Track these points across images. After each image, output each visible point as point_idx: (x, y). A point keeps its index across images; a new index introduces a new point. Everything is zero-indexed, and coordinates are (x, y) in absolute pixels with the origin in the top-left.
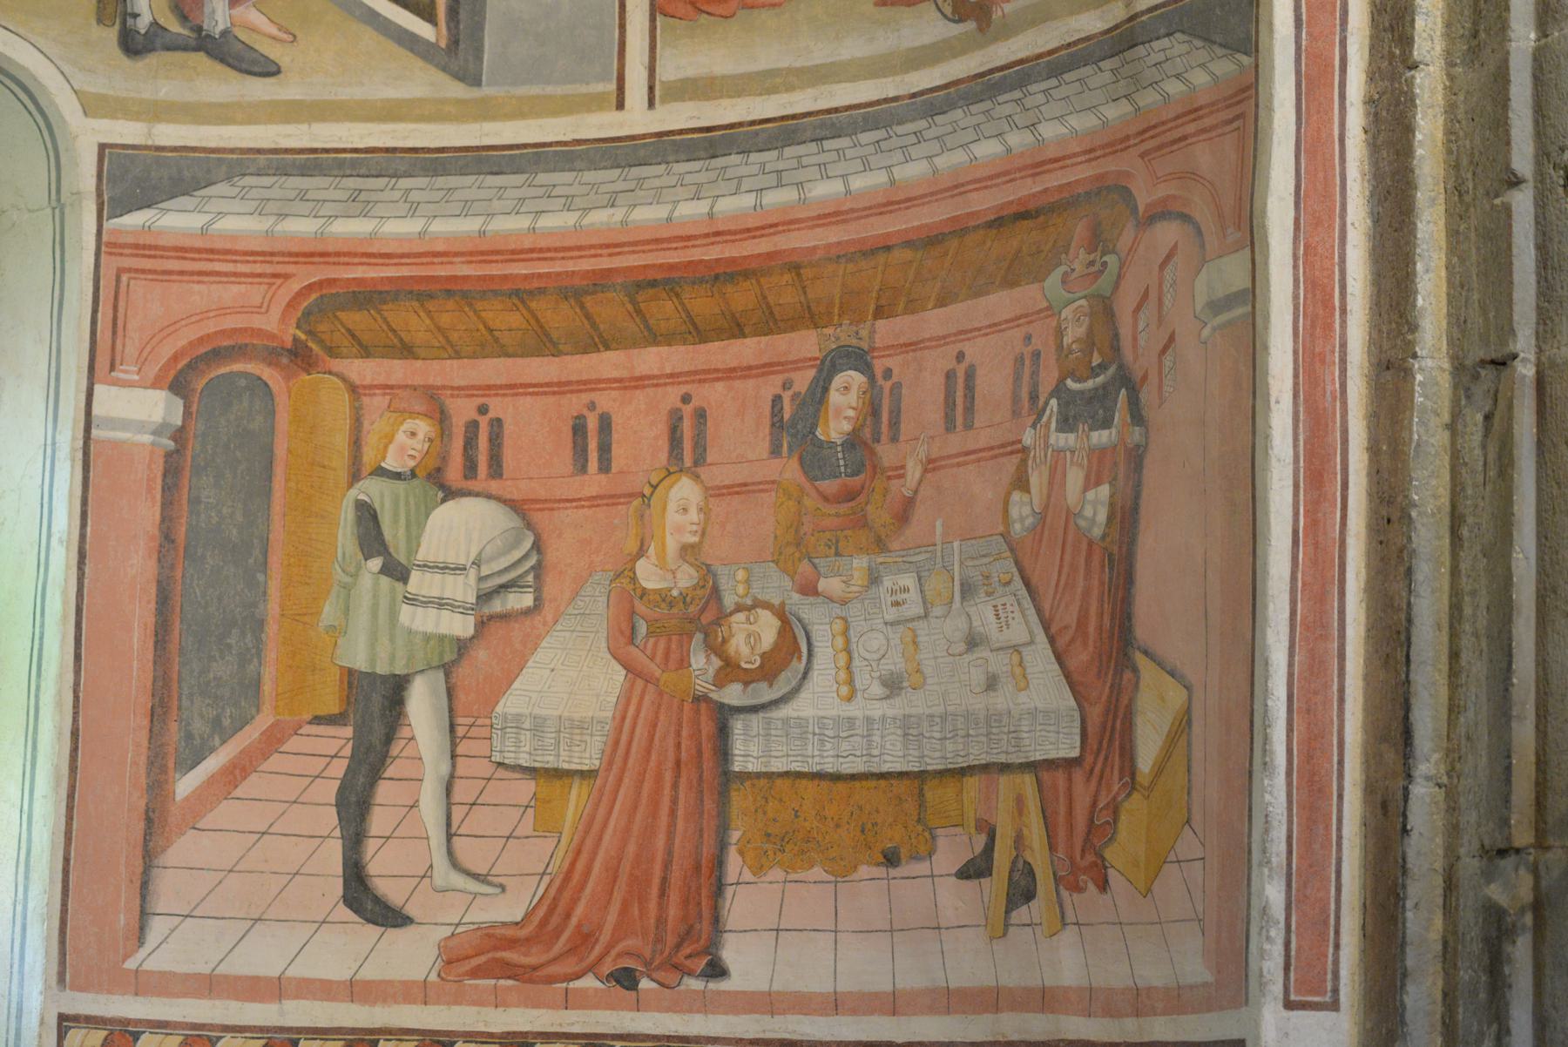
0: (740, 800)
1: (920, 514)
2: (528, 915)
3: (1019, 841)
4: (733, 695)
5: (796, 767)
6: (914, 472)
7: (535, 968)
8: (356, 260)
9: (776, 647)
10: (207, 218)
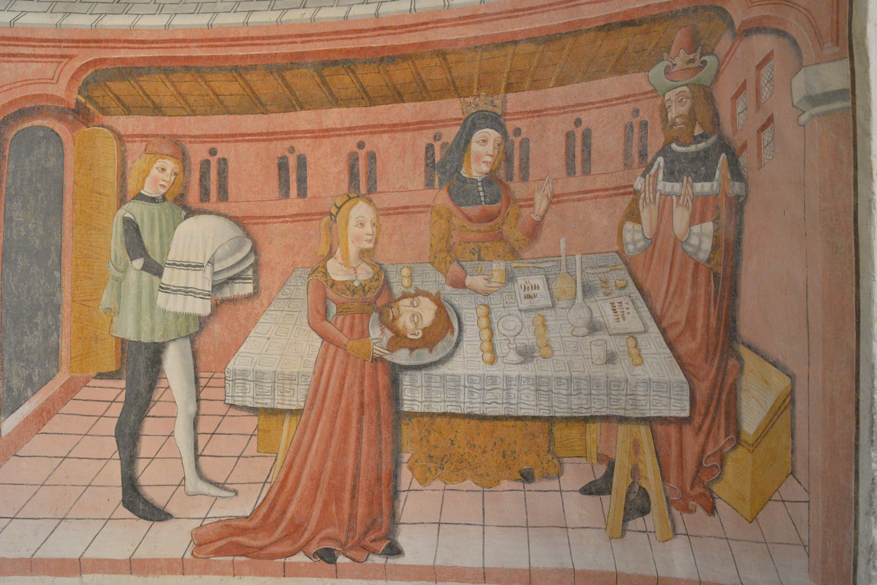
0: (408, 432)
1: (546, 234)
2: (255, 512)
3: (635, 472)
4: (402, 357)
5: (451, 409)
6: (541, 204)
7: (261, 548)
8: (120, 45)
9: (434, 323)
10: (14, 15)
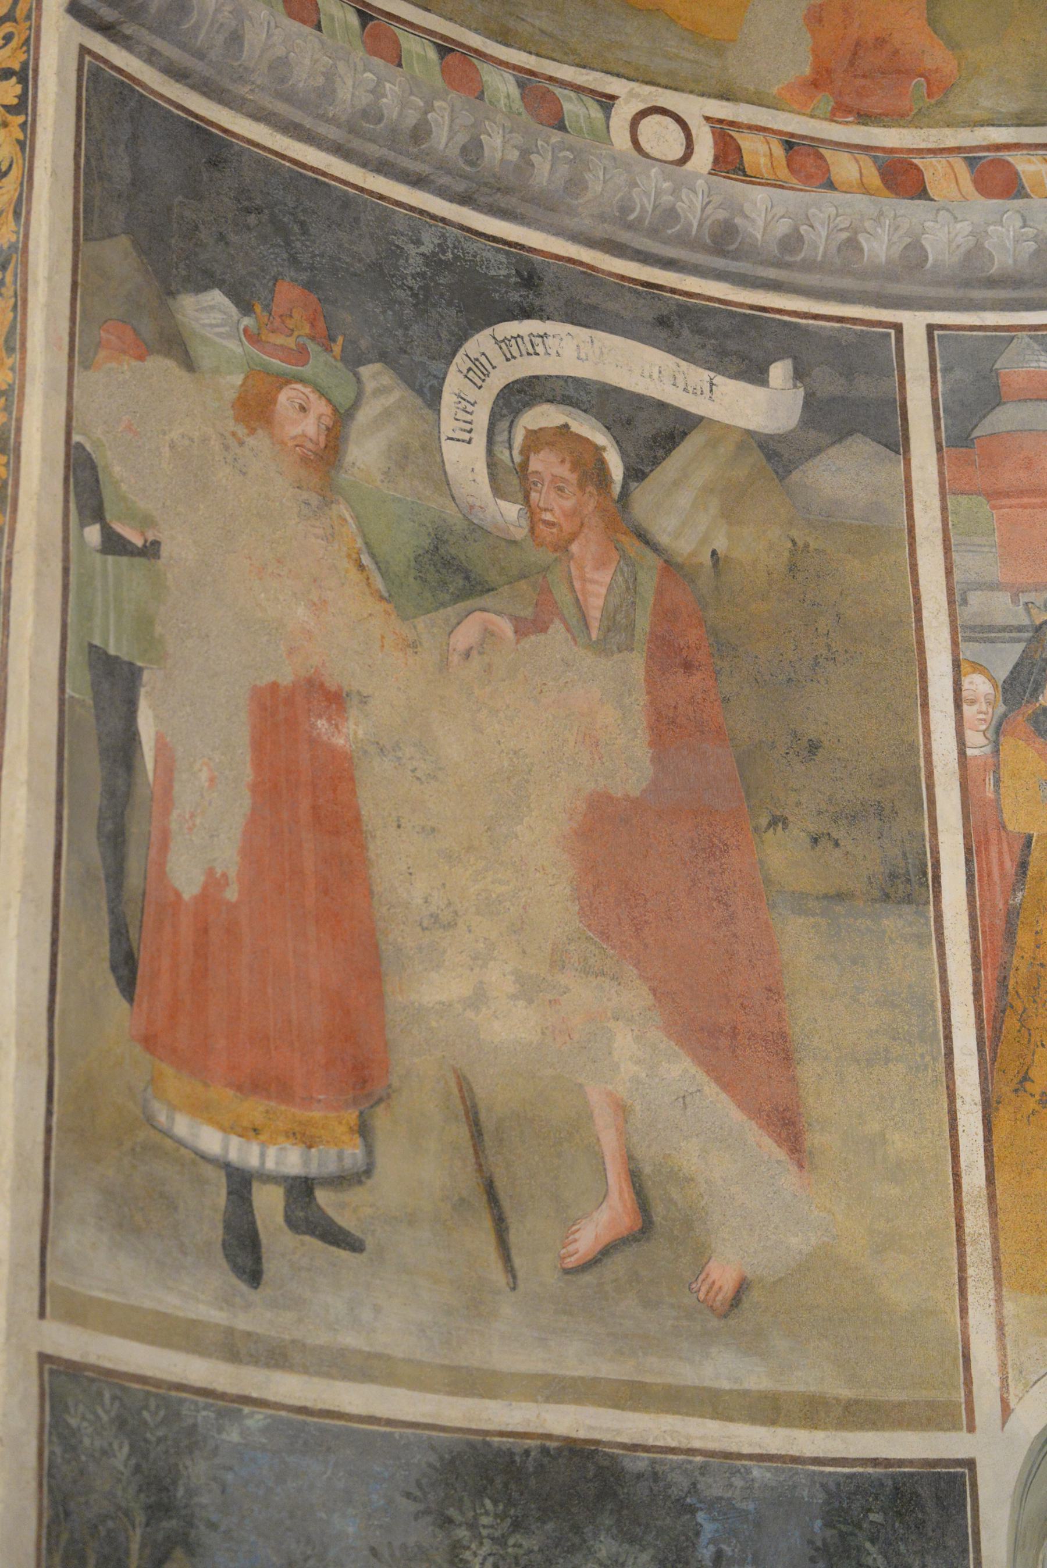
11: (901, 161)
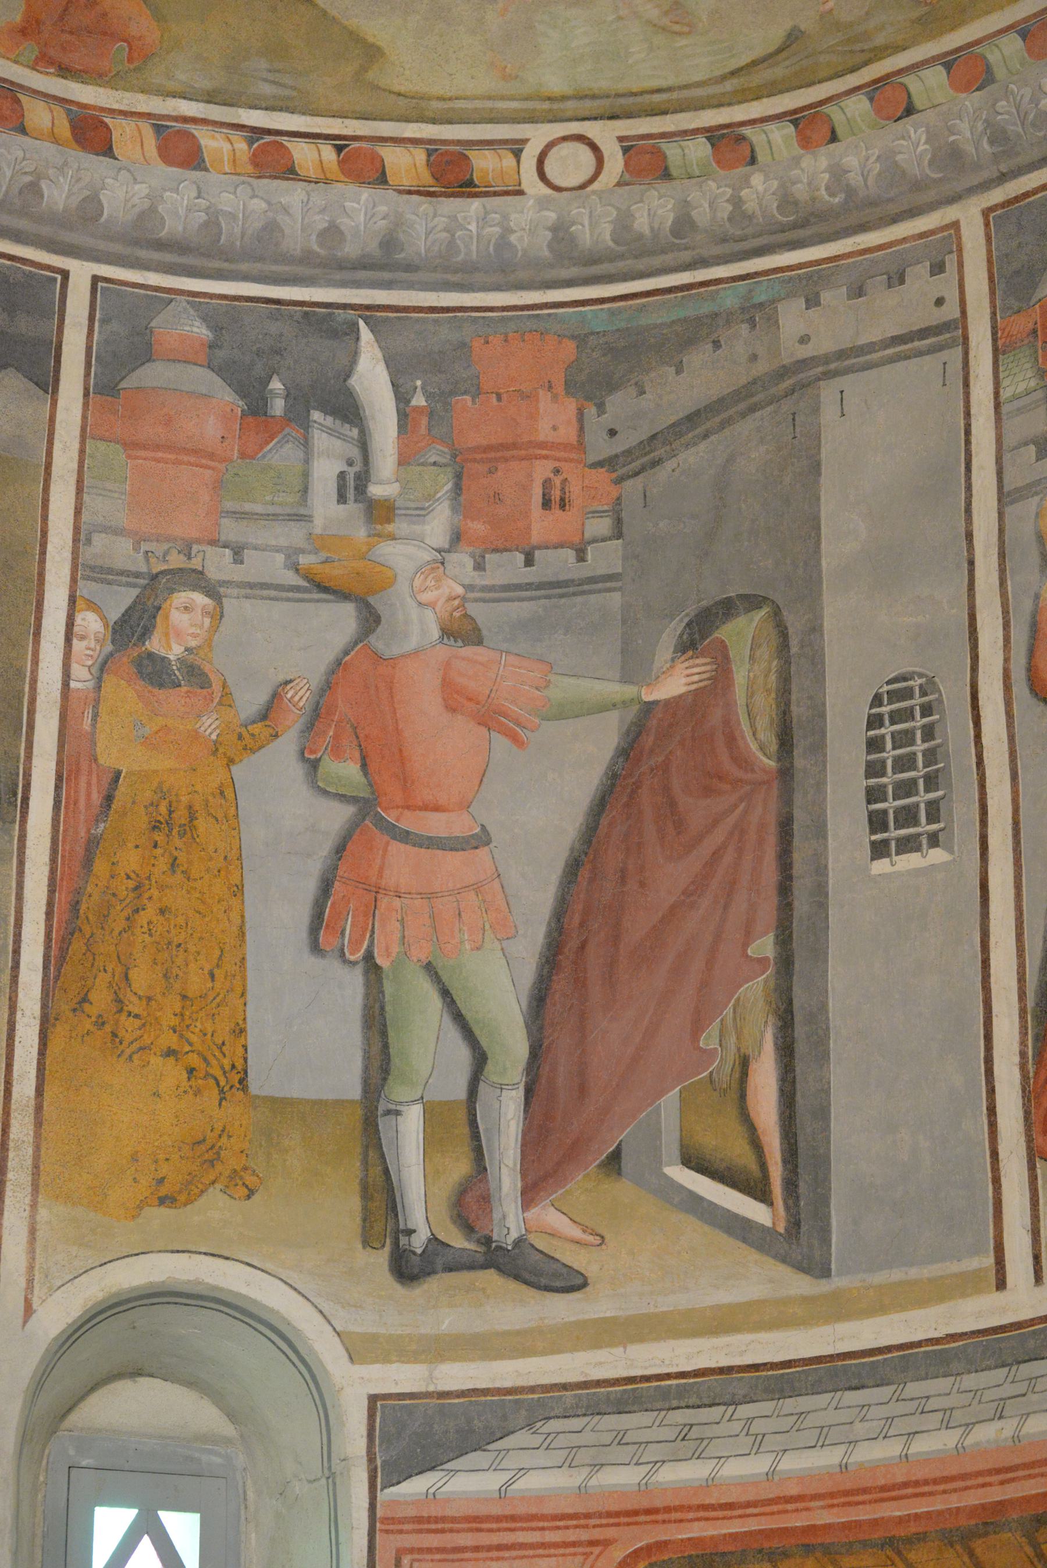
8: (691, 1515)
10: (505, 1477)
11: (92, 117)
